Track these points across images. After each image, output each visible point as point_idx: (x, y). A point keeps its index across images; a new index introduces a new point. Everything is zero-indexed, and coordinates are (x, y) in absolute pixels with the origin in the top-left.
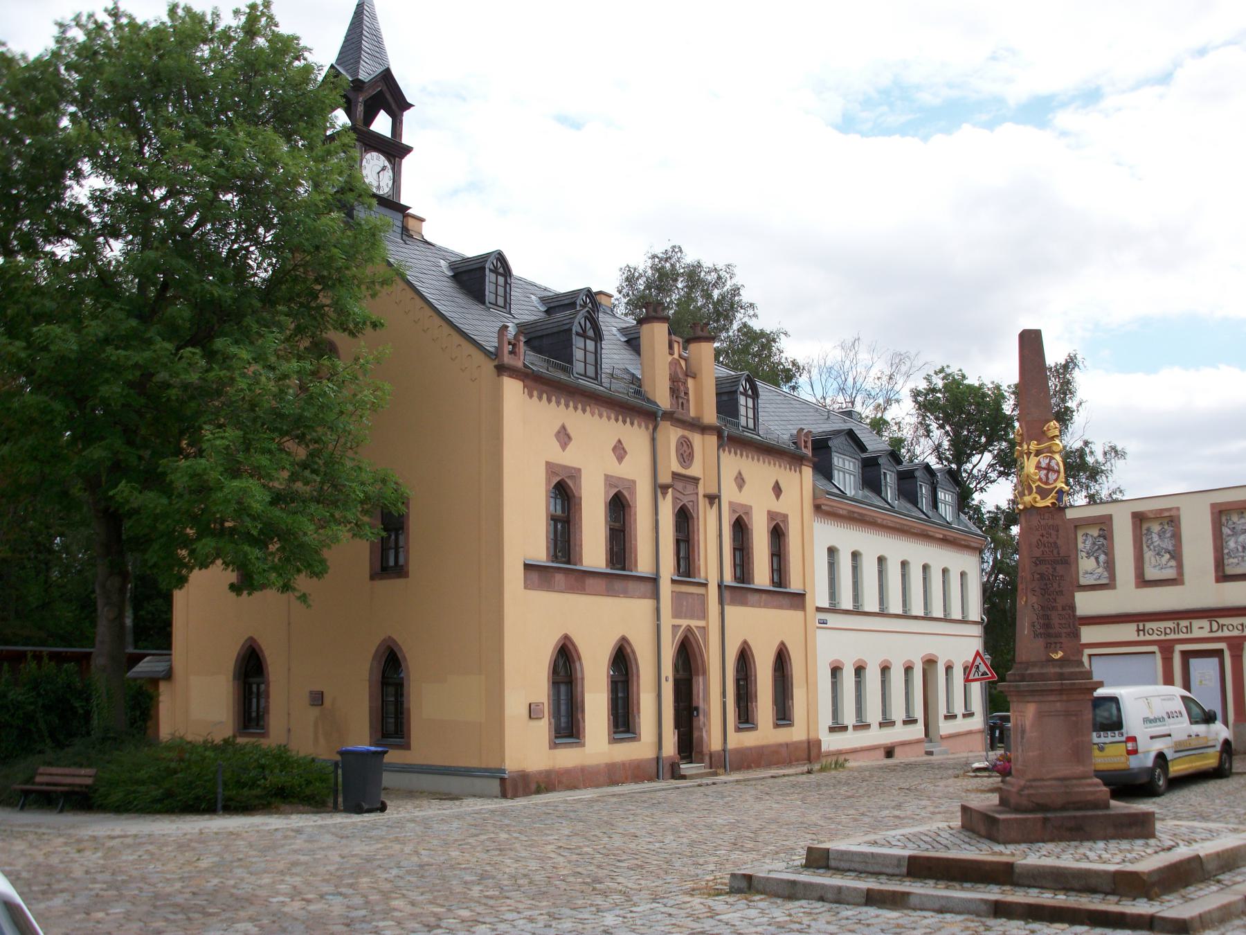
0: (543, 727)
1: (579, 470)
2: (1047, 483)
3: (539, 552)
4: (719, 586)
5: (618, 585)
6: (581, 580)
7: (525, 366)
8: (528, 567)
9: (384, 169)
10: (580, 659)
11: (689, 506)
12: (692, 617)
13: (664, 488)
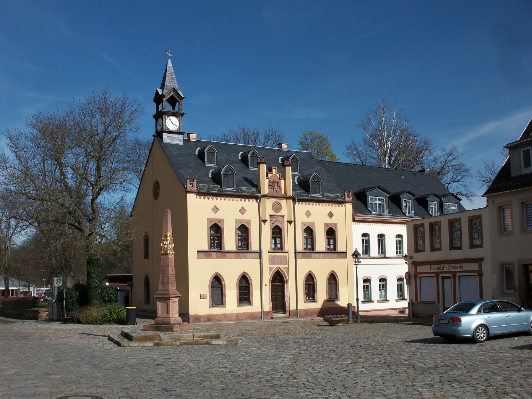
0: (207, 301)
1: (223, 219)
3: (205, 246)
5: (241, 255)
8: (198, 252)
10: (223, 280)
12: (280, 264)
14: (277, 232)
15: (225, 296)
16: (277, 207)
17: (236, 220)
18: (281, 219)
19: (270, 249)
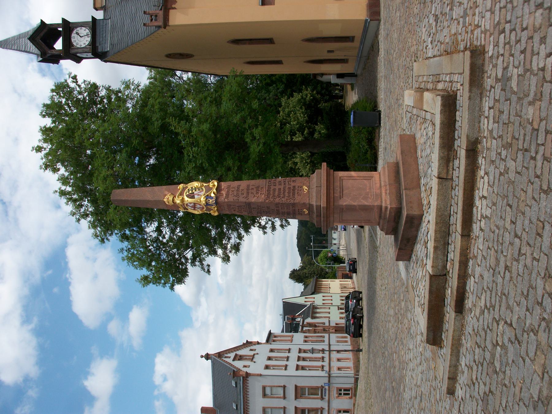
2: (203, 208)
7: (161, 9)
9: (78, 34)
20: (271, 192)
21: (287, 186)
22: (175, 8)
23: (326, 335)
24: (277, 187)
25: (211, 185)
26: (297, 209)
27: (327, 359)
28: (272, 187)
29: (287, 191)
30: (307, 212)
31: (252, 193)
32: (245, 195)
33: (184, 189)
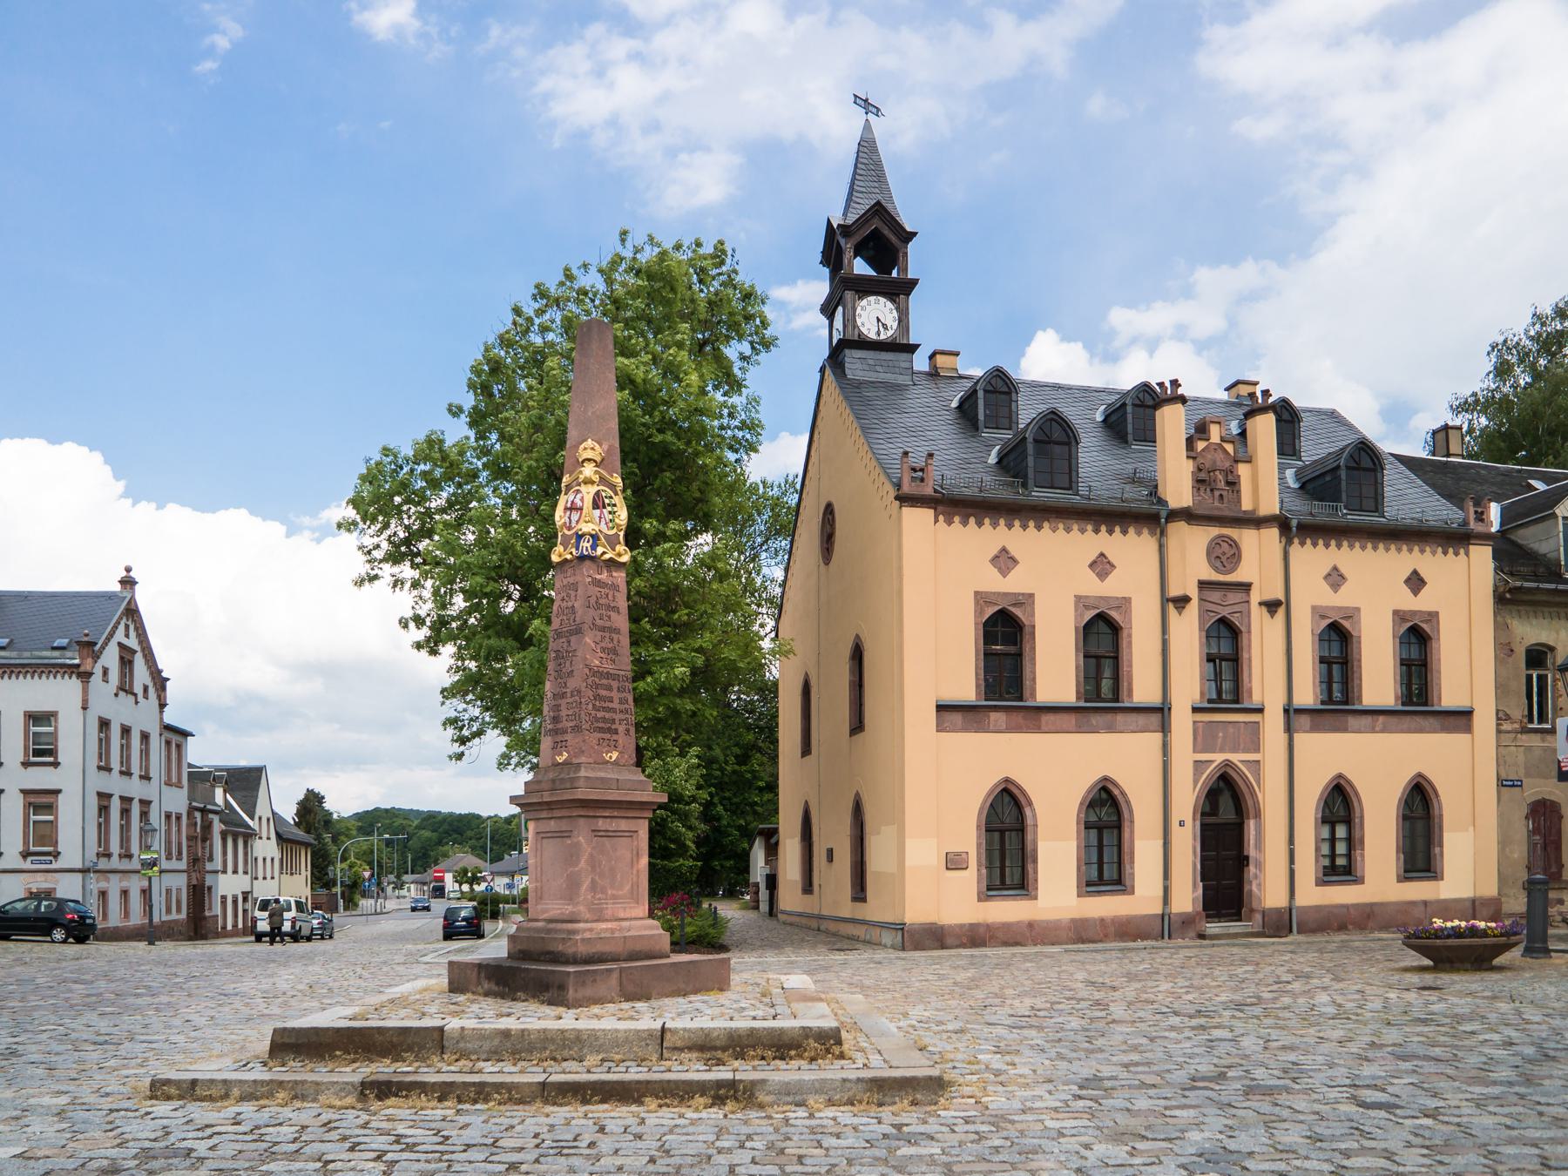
1: (1032, 596)
2: (569, 528)
3: (966, 689)
4: (1286, 711)
6: (1037, 716)
8: (942, 708)
11: (1235, 619)
13: (1182, 602)
14: (1226, 648)
15: (1035, 861)
16: (1224, 555)
17: (1078, 598)
18: (1239, 597)
19: (1197, 696)
20: (604, 681)
21: (617, 717)
22: (936, 521)
23: (183, 865)
24: (615, 694)
25: (621, 548)
26: (568, 737)
27: (125, 865)
28: (615, 684)
29: (607, 715)
30: (560, 759)
31: (603, 638)
32: (599, 622)
33: (613, 487)
